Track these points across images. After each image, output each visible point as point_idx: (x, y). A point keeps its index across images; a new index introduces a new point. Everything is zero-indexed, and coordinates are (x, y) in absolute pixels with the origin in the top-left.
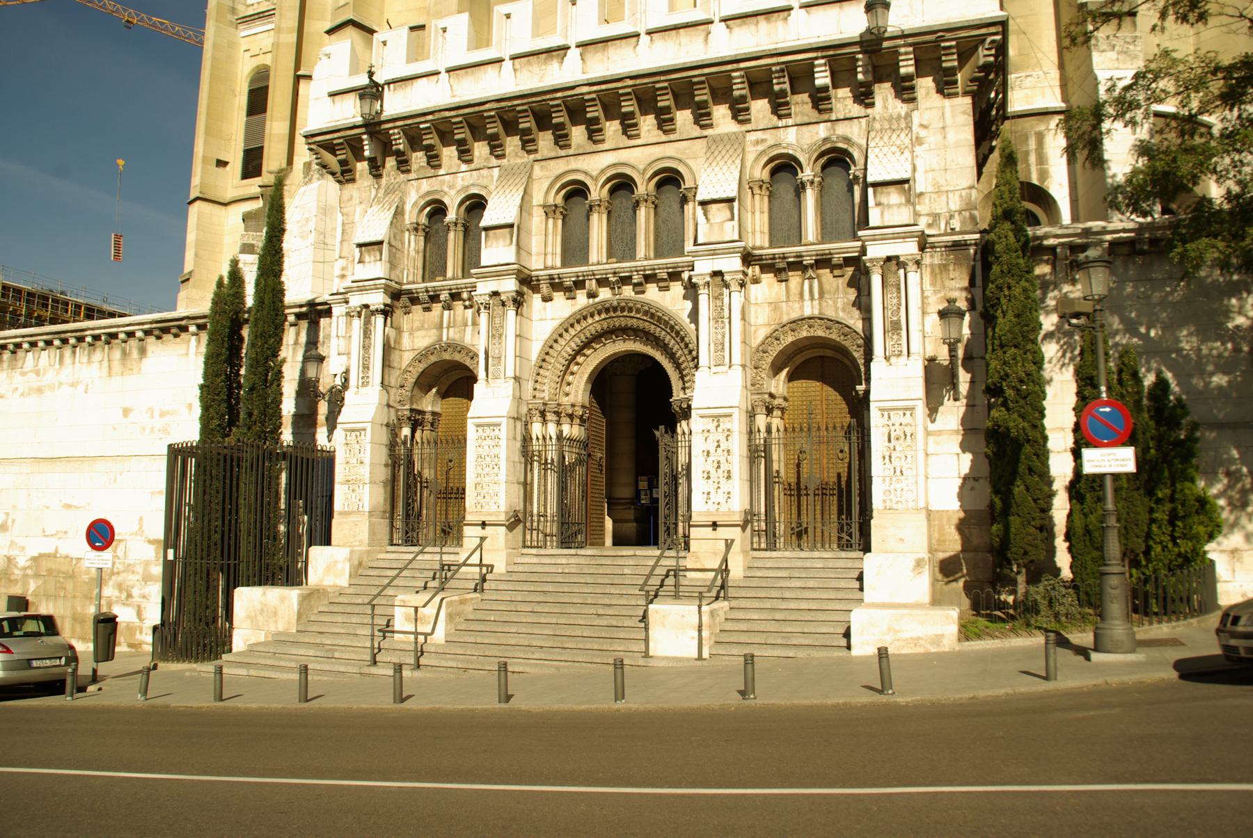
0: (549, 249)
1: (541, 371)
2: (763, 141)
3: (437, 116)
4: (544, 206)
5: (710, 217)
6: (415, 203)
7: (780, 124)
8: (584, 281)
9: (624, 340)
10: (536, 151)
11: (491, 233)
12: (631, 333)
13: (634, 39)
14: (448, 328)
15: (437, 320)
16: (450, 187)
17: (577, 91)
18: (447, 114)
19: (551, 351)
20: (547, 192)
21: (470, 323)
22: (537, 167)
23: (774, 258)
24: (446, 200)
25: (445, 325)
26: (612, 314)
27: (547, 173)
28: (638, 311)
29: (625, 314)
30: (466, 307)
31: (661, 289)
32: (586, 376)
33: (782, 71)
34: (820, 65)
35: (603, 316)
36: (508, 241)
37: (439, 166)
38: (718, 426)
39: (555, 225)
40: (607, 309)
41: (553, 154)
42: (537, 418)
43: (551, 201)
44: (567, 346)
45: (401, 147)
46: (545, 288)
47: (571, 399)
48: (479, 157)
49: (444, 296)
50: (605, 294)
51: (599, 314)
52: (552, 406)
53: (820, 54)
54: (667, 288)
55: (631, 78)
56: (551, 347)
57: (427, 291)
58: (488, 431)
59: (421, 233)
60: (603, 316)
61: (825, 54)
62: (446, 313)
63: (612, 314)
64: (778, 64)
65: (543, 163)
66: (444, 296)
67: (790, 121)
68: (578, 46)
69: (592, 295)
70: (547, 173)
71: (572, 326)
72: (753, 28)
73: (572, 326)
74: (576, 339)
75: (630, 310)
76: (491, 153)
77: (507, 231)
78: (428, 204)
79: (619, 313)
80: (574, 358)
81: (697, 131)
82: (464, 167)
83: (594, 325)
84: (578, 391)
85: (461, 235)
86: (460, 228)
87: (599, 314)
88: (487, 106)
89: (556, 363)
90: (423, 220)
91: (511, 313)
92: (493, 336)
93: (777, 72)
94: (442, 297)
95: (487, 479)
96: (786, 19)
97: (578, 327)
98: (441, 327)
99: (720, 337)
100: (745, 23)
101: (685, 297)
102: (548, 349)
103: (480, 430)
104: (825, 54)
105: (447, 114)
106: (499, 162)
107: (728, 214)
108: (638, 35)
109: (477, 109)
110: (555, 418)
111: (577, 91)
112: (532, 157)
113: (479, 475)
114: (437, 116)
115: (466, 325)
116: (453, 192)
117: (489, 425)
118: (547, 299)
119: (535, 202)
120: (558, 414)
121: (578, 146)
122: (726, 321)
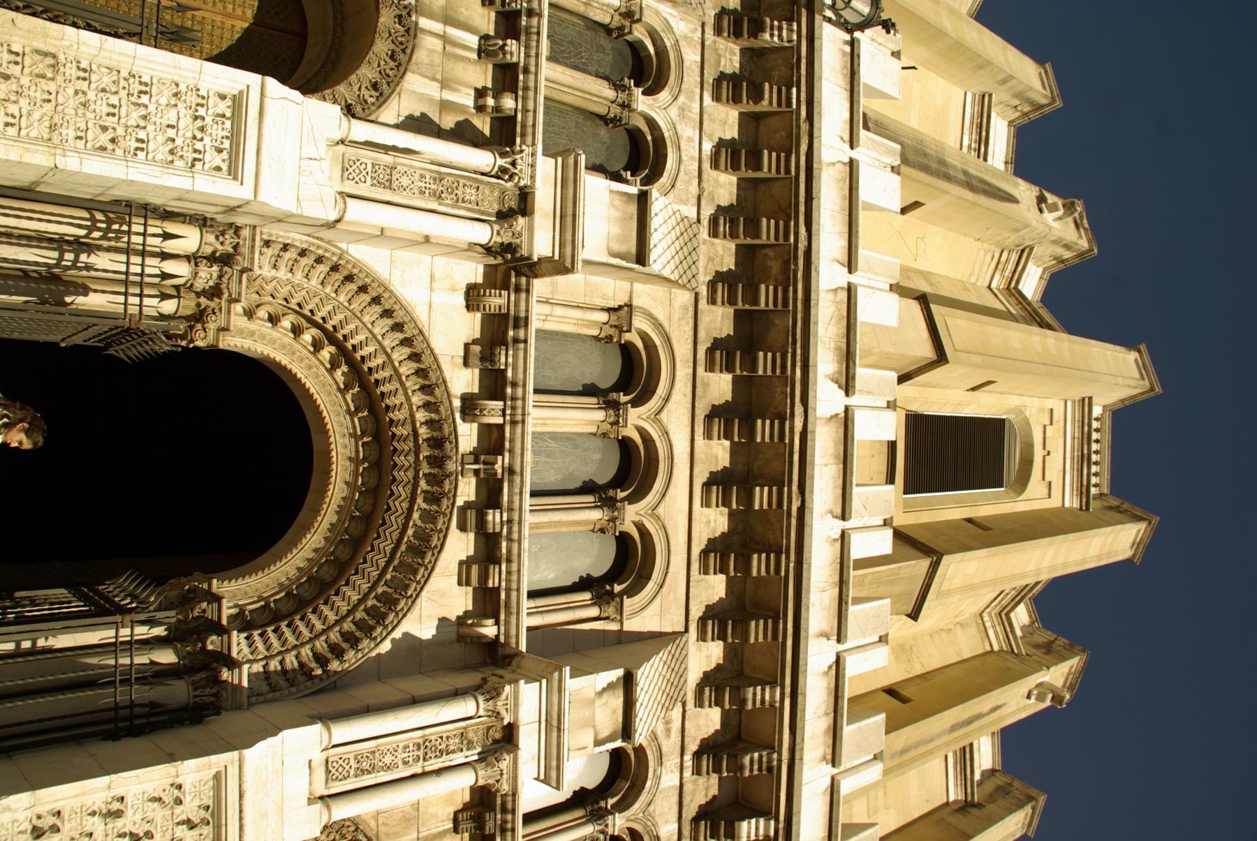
0: (559, 311)
1: (323, 269)
2: (668, 730)
3: (804, 127)
4: (630, 306)
5: (605, 695)
6: (670, 28)
7: (688, 757)
8: (501, 396)
9: (355, 461)
10: (712, 301)
11: (633, 209)
12: (373, 482)
13: (839, 511)
14: (444, 38)
15: (463, 13)
16: (682, 109)
17: (799, 409)
18: (804, 148)
19: (366, 298)
20: (658, 325)
21: (448, 96)
22: (685, 297)
23: (504, 810)
24: (664, 95)
25: (452, 32)
26: (425, 452)
27: (676, 317)
28: (429, 517)
29: (423, 484)
30: (480, 93)
31: (465, 565)
32: (284, 360)
33: (770, 769)
34: (767, 828)
35: (423, 431)
36: (616, 247)
37: (717, 98)
38: (191, 825)
39: (593, 324)
40: (440, 442)
41: (702, 334)
42: (211, 243)
43: (639, 323)
44: (369, 334)
45: (767, 36)
46: (496, 301)
47: (238, 320)
48: (716, 181)
49: (514, 50)
50: (467, 436)
51: (429, 423)
52: (232, 285)
53: (781, 825)
54: (463, 580)
55: (802, 510)
56: (376, 300)
57: (530, 13)
58: (219, 131)
59: (617, 21)
60: (423, 431)
61: (781, 832)
62: (473, 41)
63: (425, 452)
64: (780, 760)
65: (691, 309)
66: (514, 50)
67: (688, 774)
68: (847, 409)
69: (470, 406)
70: (676, 317)
71: (415, 357)
72: (822, 709)
73: (415, 357)
74: (380, 360)
75: (434, 498)
76: (719, 208)
77: (632, 248)
78: (661, 52)
79: (425, 468)
80: (333, 341)
81: (697, 611)
82: (708, 147)
83: (406, 405)
84: (247, 335)
85: (602, 110)
86: (615, 110)
87: (429, 423)
88: (802, 230)
89: (335, 305)
90: (639, 33)
91: (482, 234)
92: (440, 178)
93: (770, 760)
94: (512, 45)
95: (70, 102)
96: (824, 758)
97: (406, 369)
98: (448, 20)
99: (388, 759)
100: (829, 694)
101: (443, 621)
102: (409, 331)
103: (224, 107)
104: (781, 832)
105: (804, 148)
106: (705, 222)
107: (604, 733)
108: (844, 516)
109: (802, 208)
110: (199, 285)
111: (799, 409)
112: (703, 290)
113: (86, 74)
114: (804, 127)
115: (445, 84)
116: (673, 112)
117: (236, 137)
118: (473, 296)
119: (638, 287)
120: (214, 292)
121: (706, 385)
122: (418, 769)
